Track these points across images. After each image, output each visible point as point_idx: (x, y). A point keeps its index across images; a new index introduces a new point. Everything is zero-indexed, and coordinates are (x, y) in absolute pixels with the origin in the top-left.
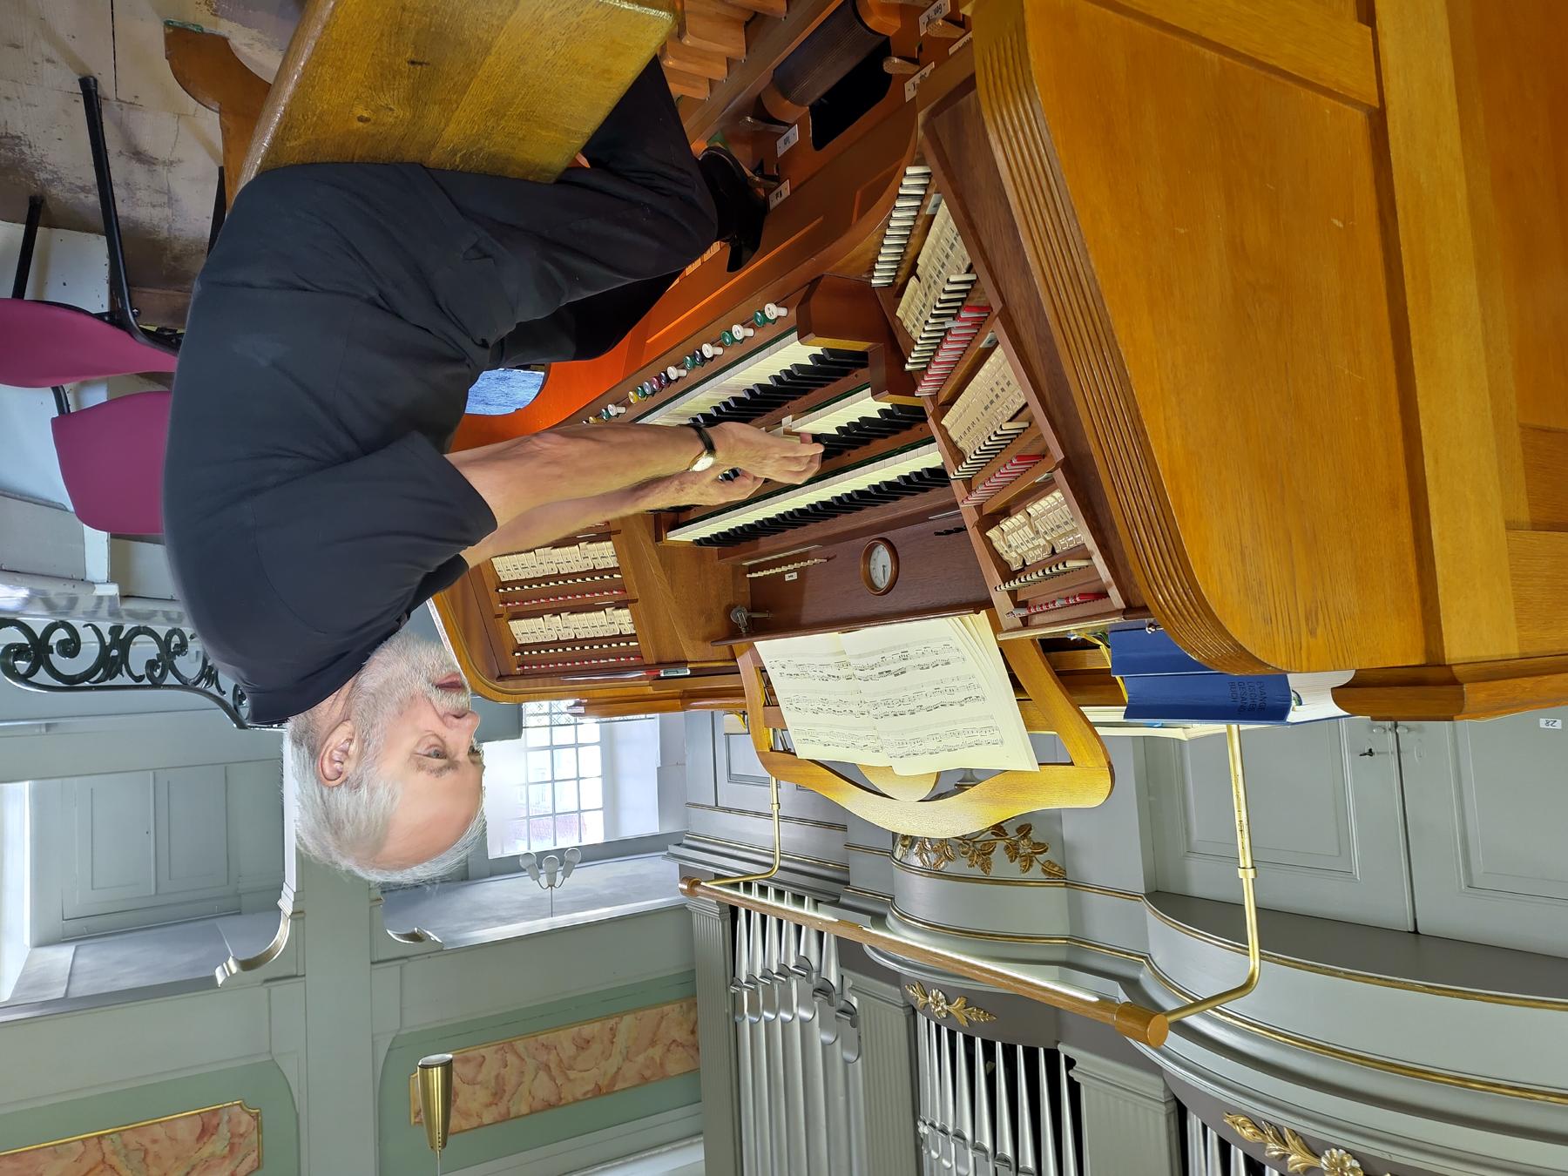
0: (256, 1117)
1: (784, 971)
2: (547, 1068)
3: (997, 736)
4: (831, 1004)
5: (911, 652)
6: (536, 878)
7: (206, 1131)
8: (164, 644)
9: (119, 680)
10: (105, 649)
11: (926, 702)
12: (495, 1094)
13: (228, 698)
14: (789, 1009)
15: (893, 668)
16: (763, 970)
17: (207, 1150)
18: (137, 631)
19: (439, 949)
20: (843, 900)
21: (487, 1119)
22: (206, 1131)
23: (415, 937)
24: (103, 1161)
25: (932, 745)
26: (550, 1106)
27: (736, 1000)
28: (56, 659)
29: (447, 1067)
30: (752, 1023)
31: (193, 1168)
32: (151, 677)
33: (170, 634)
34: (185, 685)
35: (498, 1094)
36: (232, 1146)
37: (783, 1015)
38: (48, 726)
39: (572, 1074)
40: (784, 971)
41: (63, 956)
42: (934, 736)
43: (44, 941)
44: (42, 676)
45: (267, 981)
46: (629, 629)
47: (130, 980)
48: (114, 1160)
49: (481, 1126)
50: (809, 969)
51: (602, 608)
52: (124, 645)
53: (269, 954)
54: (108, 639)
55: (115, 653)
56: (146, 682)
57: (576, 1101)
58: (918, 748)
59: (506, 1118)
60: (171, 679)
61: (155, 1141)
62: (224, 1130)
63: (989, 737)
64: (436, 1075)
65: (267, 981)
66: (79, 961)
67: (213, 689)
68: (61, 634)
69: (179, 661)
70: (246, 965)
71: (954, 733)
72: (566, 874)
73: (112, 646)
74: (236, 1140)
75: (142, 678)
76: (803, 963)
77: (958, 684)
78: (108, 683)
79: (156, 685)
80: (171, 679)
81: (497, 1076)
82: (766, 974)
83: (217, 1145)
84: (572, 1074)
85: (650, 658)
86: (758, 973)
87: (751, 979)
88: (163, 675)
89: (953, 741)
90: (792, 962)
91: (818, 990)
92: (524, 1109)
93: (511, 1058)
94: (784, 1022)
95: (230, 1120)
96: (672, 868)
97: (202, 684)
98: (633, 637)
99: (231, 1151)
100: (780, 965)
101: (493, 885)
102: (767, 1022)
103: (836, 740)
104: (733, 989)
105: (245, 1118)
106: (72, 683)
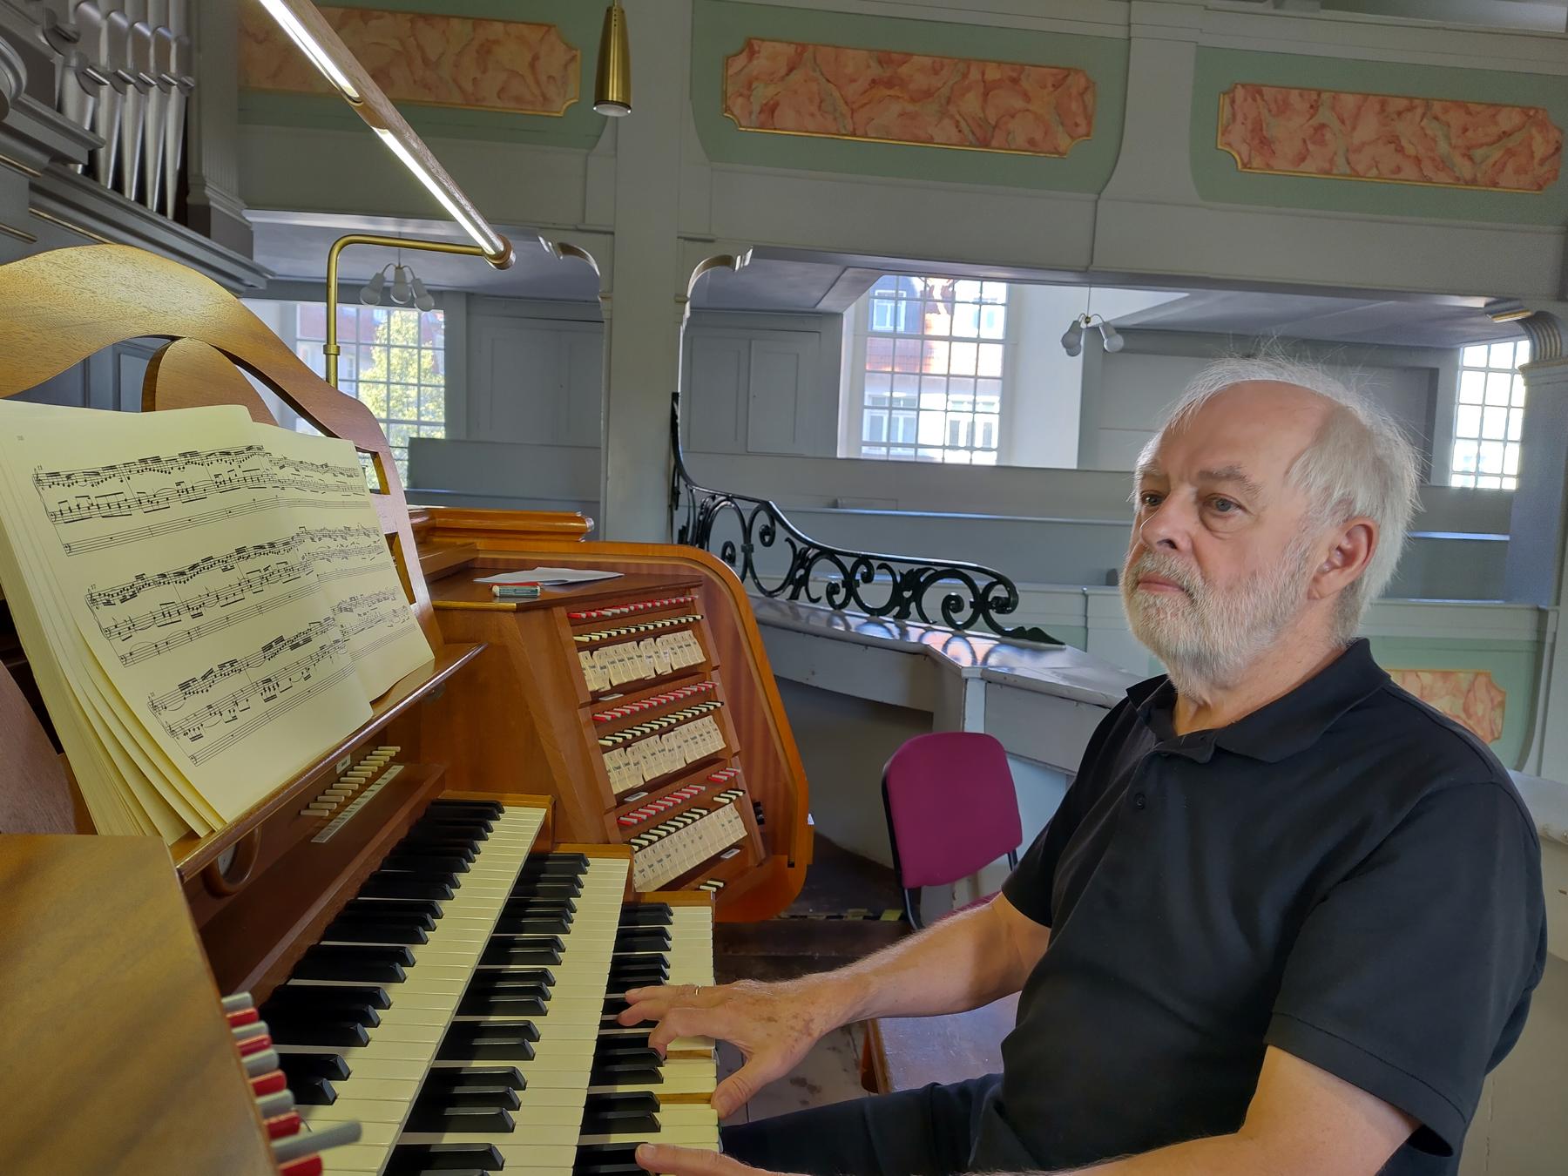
0: (728, 109)
1: (119, 84)
2: (426, 61)
3: (56, 495)
4: (52, 16)
5: (257, 701)
6: (416, 281)
7: (771, 109)
8: (852, 592)
9: (905, 568)
10: (917, 598)
11: (213, 580)
12: (489, 52)
13: (781, 533)
14: (114, 29)
15: (287, 656)
16: (147, 93)
17: (771, 91)
18: (884, 611)
19: (545, 229)
20: (44, 159)
21: (499, 27)
22: (771, 109)
23: (566, 249)
24: (853, 111)
25: (194, 475)
26: (427, 18)
27: (186, 65)
28: (968, 597)
29: (601, 99)
30: (166, 27)
31: (782, 79)
32: (870, 567)
33: (844, 604)
34: (830, 554)
35: (485, 51)
36: (749, 86)
37: (122, 22)
38: (835, 505)
39: (399, 48)
40: (119, 84)
41: (826, 305)
42: (185, 493)
43: (838, 316)
44: (981, 583)
45: (711, 241)
46: (583, 655)
47: (794, 269)
48: (844, 109)
49: (506, 22)
50: (81, 75)
51: (615, 689)
52: (896, 599)
53: (706, 266)
54: (913, 605)
55: (907, 594)
56: (875, 564)
57: (393, 13)
58: (221, 468)
59: (478, 22)
60: (849, 563)
61: (812, 115)
62: (756, 108)
63: (69, 494)
64: (613, 94)
65: (711, 241)
66: (817, 294)
67: (800, 546)
68: (960, 618)
69: (837, 577)
70: (727, 261)
71: (152, 503)
72: (380, 277)
73: (909, 601)
74: (746, 92)
75: (880, 567)
76: (90, 86)
77: (157, 634)
78: (916, 567)
79: (864, 560)
80: (849, 563)
81: (484, 72)
82: (143, 87)
83: (763, 93)
84: (399, 48)
85: (560, 612)
86: (154, 92)
87: (165, 86)
88: (855, 567)
89: (150, 482)
90: (105, 91)
91: (68, 39)
92: (455, 22)
93: (469, 87)
94: (121, 11)
95: (751, 113)
96: (259, 259)
97: (812, 553)
98: (581, 647)
99: (750, 84)
100: (124, 93)
101: (442, 282)
102: (145, 21)
103: (316, 476)
104: (190, 81)
105: (737, 111)
106: (953, 572)
